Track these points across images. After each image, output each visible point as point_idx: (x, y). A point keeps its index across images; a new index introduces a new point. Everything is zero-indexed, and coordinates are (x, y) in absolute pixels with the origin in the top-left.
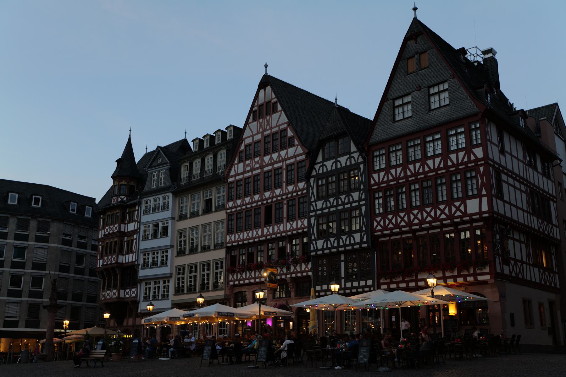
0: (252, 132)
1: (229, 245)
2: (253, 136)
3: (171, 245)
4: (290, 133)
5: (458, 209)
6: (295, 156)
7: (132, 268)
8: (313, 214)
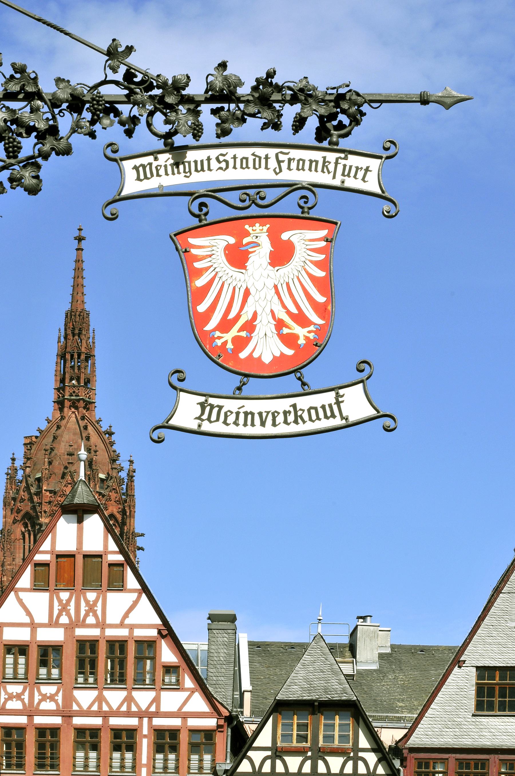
0: (29, 613)
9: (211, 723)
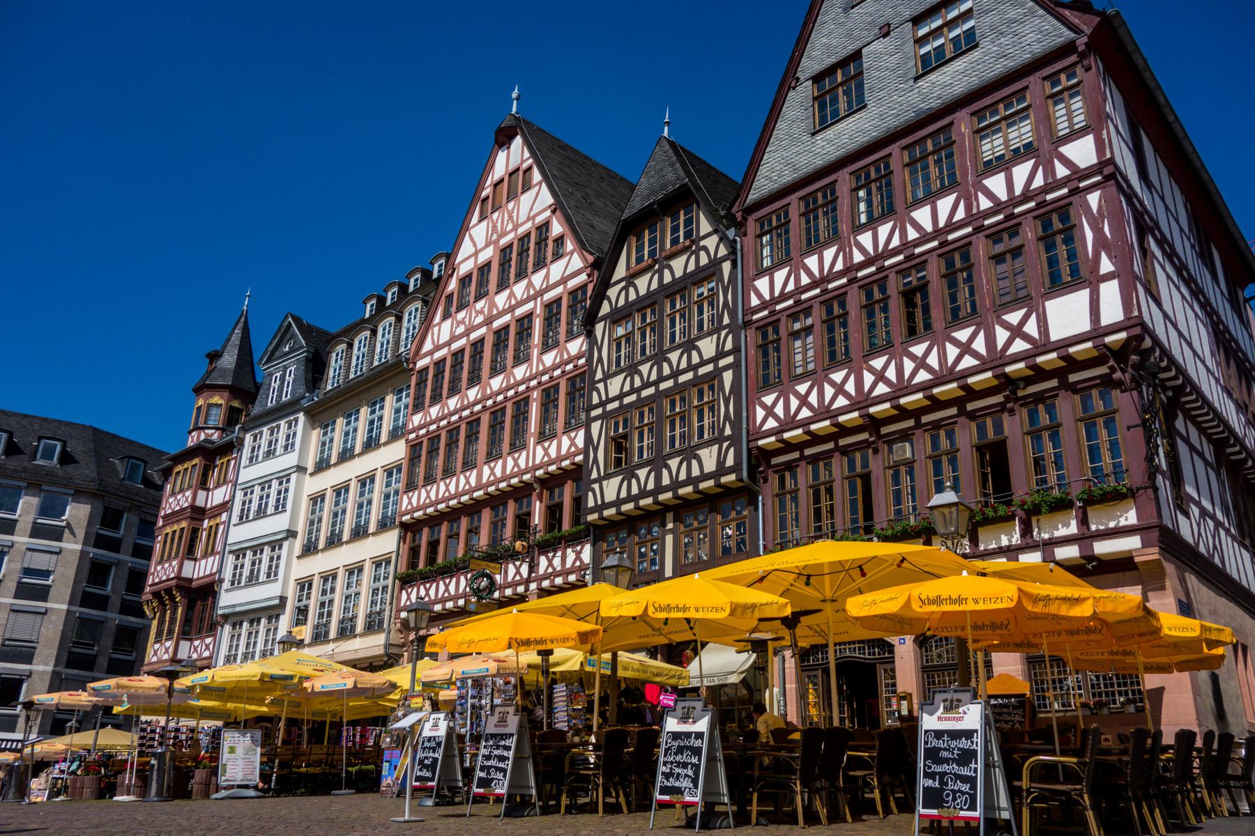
0: (475, 245)
1: (406, 518)
2: (476, 254)
3: (288, 531)
4: (557, 228)
5: (1017, 332)
6: (564, 281)
7: (207, 591)
8: (599, 411)
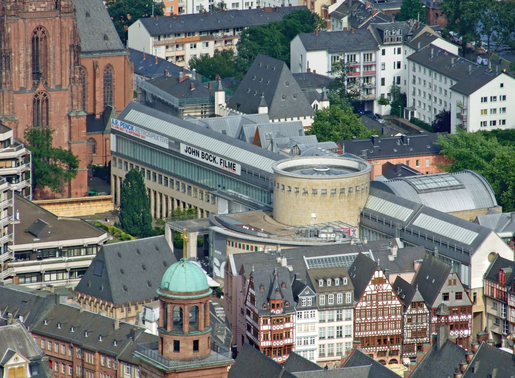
9: (400, 305)
